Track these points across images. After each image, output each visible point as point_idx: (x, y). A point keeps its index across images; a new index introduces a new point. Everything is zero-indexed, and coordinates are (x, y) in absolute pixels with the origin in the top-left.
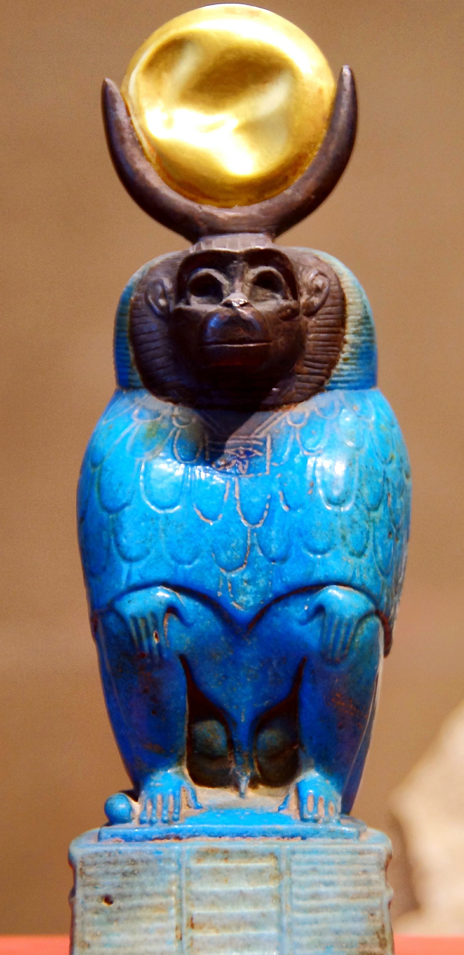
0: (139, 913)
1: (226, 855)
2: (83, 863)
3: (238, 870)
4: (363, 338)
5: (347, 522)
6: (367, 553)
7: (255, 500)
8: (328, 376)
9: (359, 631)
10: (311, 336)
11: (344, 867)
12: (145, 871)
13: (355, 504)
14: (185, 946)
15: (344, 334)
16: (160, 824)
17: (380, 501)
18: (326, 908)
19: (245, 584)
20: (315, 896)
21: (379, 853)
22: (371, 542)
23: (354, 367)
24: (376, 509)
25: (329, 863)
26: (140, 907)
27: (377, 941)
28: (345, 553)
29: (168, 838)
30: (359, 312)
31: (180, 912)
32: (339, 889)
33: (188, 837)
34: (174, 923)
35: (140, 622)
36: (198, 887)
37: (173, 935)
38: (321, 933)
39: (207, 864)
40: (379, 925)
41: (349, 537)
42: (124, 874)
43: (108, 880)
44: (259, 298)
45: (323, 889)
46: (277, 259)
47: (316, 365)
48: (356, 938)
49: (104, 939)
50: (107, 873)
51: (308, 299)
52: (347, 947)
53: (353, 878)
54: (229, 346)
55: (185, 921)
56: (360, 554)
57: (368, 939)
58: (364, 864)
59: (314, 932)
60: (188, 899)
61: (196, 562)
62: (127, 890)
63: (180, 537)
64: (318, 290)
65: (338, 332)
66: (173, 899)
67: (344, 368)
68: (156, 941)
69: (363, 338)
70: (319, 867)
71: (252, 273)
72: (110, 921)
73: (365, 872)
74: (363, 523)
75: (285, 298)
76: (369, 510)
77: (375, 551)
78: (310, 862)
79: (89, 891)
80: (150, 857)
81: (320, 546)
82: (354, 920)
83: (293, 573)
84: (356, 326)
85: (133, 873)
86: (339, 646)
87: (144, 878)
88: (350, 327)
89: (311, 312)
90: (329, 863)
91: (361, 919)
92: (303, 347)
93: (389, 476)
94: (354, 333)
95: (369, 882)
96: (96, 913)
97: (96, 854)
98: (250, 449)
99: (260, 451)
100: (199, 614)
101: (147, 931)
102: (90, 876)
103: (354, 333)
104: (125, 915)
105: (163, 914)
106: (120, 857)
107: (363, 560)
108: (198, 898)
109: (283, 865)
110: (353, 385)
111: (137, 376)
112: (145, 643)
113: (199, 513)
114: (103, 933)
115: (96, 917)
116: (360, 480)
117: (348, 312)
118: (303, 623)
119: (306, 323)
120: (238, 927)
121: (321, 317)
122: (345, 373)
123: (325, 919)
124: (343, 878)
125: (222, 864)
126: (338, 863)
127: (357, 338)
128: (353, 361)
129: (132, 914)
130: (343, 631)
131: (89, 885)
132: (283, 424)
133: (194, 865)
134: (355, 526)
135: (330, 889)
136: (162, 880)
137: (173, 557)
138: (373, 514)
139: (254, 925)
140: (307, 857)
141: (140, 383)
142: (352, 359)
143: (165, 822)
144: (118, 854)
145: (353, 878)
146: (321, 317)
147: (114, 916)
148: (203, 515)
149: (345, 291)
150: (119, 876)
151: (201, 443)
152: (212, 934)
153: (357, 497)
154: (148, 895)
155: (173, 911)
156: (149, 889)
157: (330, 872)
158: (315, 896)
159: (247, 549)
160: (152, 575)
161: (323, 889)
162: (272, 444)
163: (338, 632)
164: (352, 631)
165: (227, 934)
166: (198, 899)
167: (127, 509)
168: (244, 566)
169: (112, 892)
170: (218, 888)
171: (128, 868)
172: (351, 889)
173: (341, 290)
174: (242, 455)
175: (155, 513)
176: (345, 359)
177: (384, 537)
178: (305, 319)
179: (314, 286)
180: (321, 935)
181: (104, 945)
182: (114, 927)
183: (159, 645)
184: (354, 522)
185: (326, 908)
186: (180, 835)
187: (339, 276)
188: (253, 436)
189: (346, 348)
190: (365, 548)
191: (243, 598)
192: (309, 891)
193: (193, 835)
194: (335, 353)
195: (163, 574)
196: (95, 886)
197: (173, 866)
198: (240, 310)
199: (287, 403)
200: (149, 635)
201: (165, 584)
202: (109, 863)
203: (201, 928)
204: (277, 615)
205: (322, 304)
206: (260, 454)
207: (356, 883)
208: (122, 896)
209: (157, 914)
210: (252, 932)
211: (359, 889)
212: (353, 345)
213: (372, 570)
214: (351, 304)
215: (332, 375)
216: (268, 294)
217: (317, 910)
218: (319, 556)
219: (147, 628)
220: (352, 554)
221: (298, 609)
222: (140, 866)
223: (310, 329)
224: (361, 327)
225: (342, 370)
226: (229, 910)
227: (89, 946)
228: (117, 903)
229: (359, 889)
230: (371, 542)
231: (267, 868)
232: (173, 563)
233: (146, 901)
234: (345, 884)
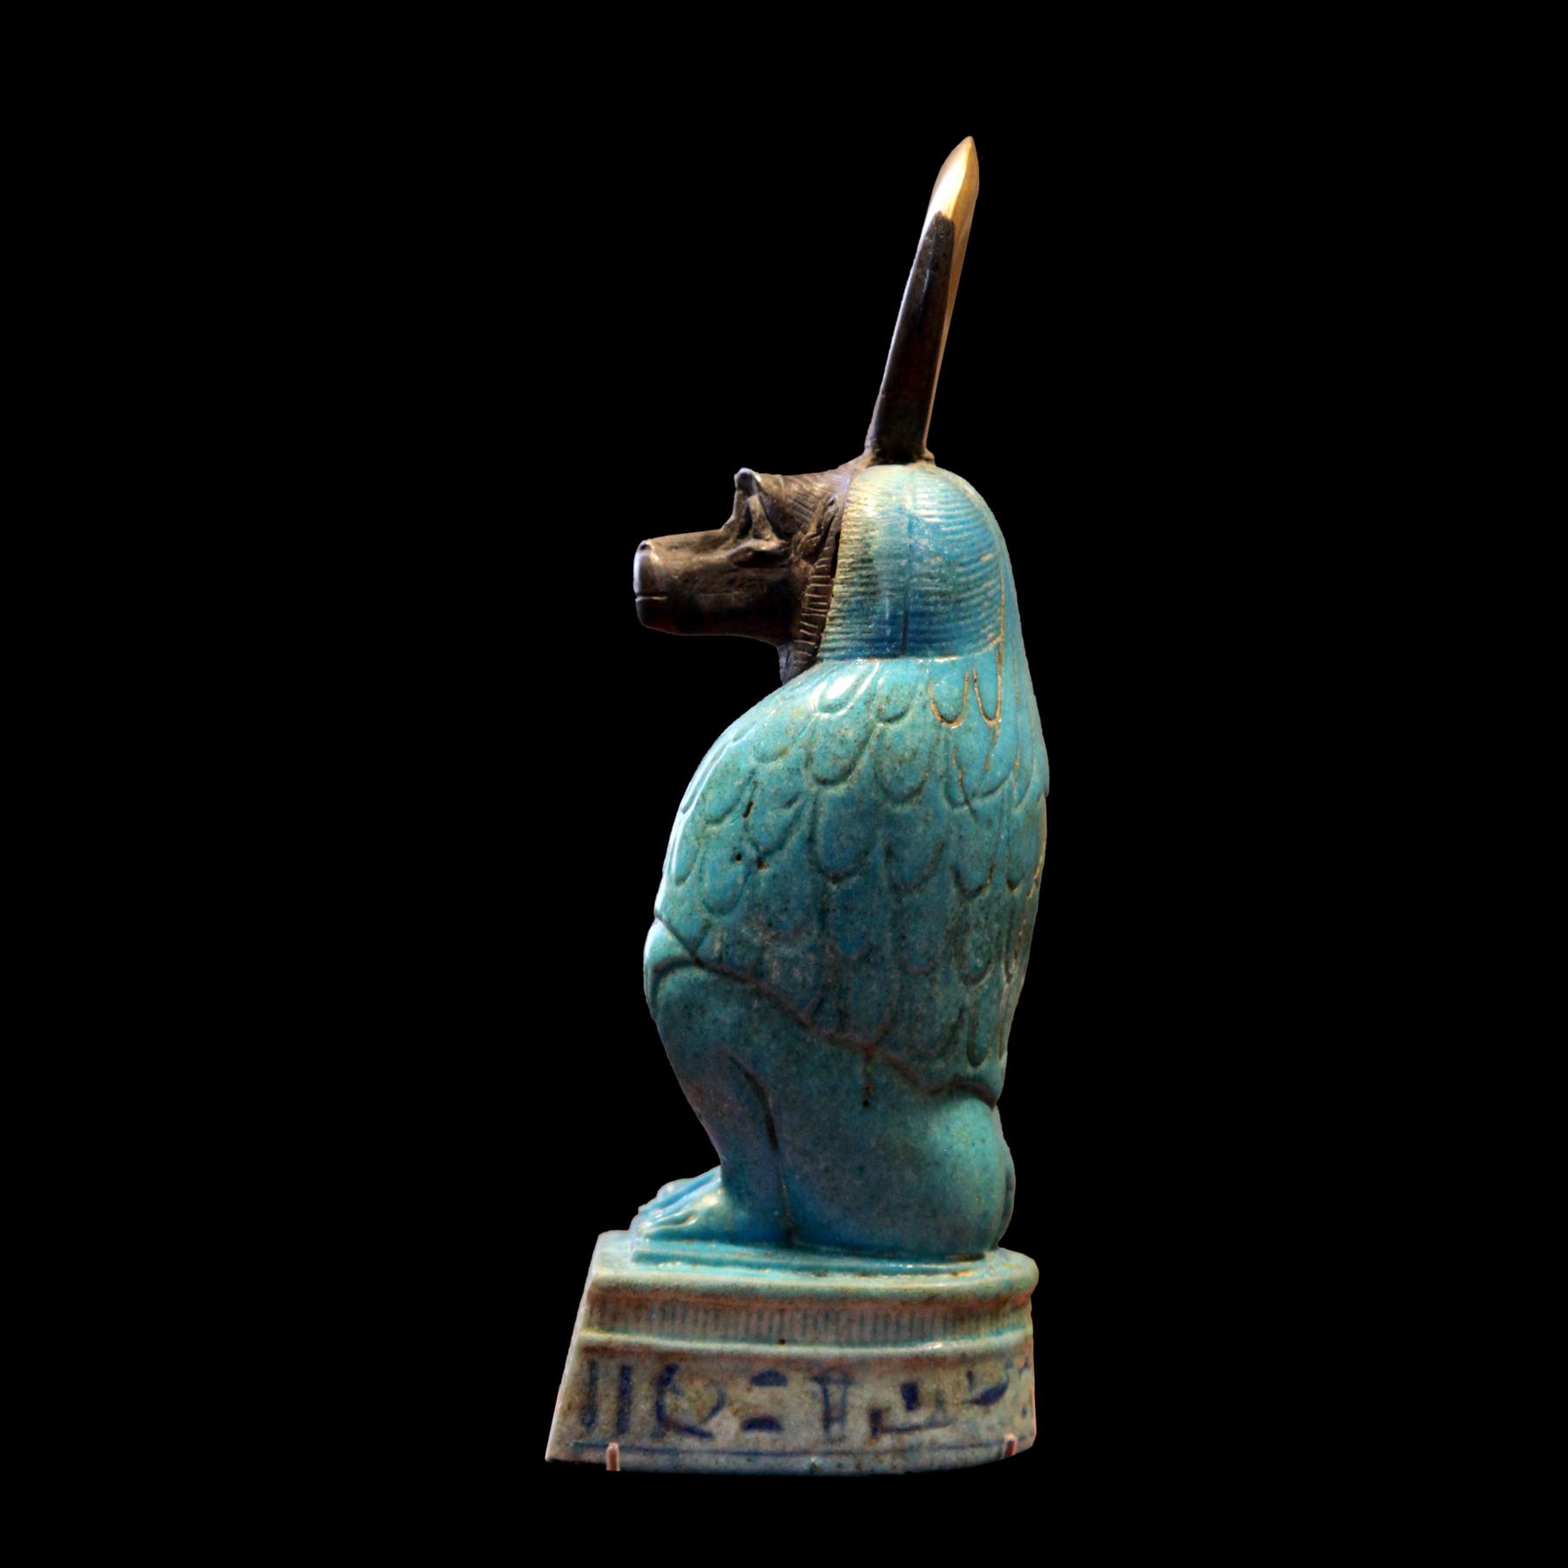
4: (853, 589)
8: (819, 642)
17: (729, 811)
22: (696, 867)
24: (718, 821)
67: (833, 634)
69: (853, 589)
76: (708, 822)
77: (701, 879)
88: (839, 576)
93: (761, 777)
107: (681, 889)
176: (832, 618)
177: (720, 861)
178: (804, 564)
212: (840, 599)
213: (687, 904)
230: (696, 867)
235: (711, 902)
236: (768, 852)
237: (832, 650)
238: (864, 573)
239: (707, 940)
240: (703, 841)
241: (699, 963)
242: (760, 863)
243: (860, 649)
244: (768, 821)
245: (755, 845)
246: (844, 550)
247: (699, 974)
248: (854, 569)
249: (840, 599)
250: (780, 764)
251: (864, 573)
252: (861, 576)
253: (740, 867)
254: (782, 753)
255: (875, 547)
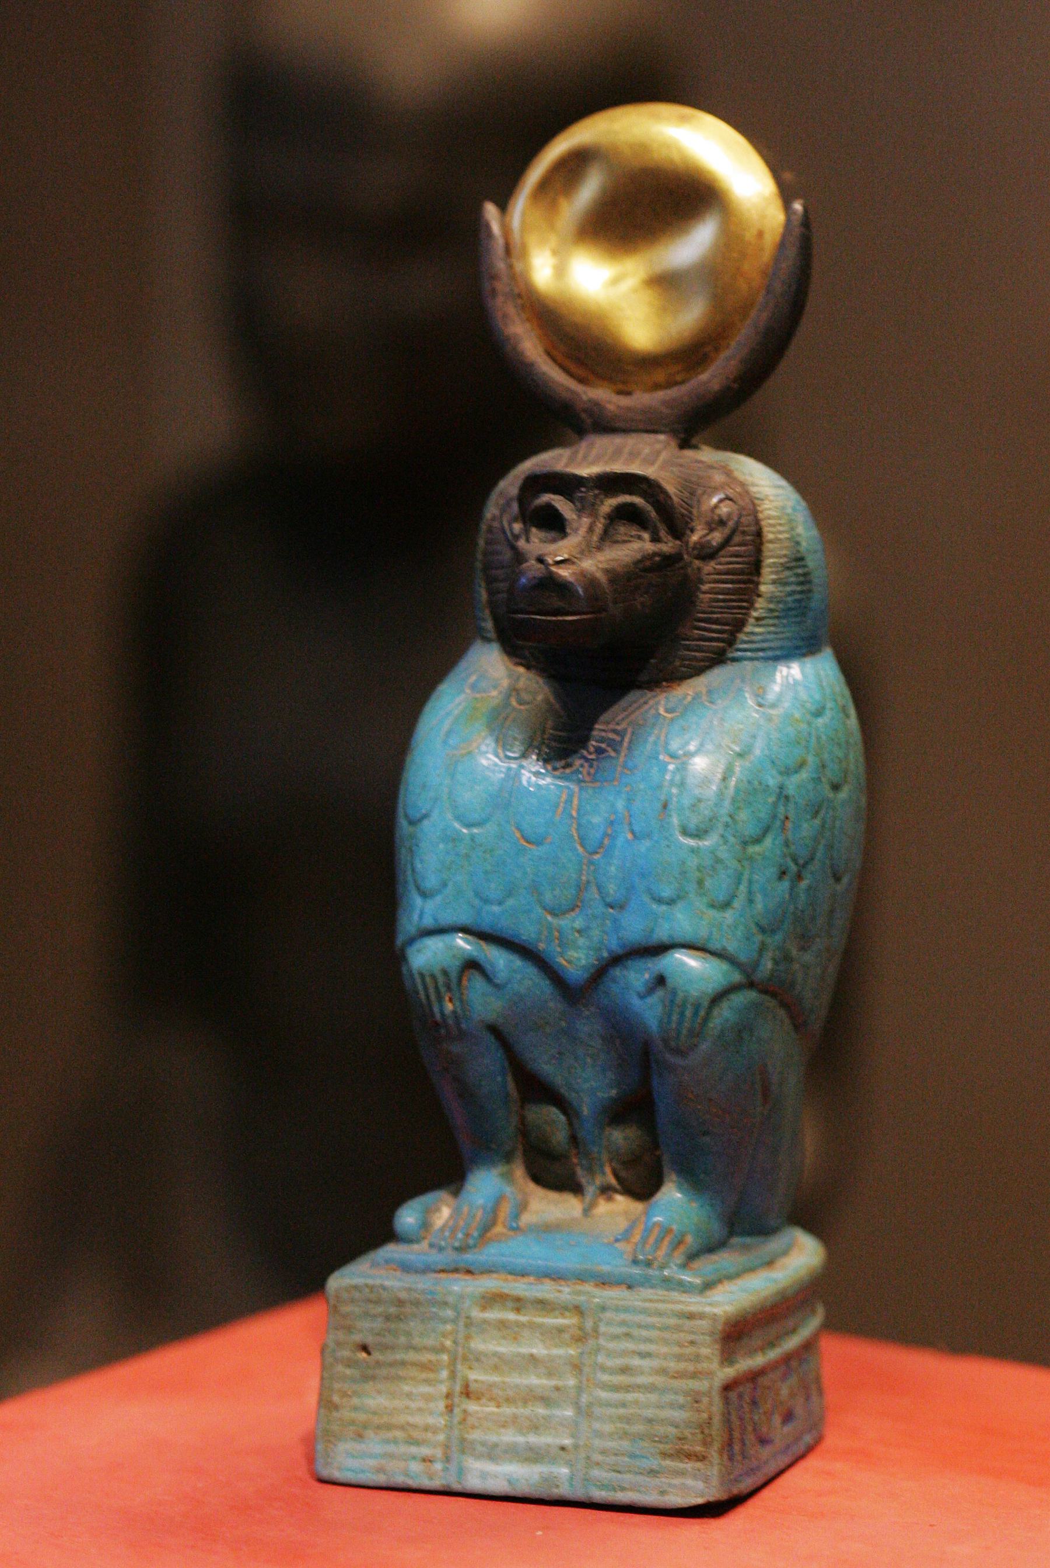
0: (401, 1372)
1: (519, 1303)
2: (337, 1297)
3: (532, 1326)
4: (789, 589)
5: (709, 862)
6: (737, 904)
7: (596, 820)
9: (716, 1012)
10: (705, 587)
11: (667, 1335)
12: (415, 1316)
13: (722, 836)
14: (456, 1420)
15: (758, 584)
16: (450, 1251)
17: (766, 830)
18: (638, 1387)
19: (577, 935)
20: (625, 1370)
21: (714, 1318)
22: (743, 888)
23: (772, 629)
24: (758, 840)
25: (647, 1327)
26: (403, 1363)
27: (700, 1436)
28: (700, 903)
29: (456, 1270)
30: (784, 552)
31: (453, 1375)
32: (655, 1363)
33: (482, 1273)
34: (444, 1389)
35: (428, 980)
36: (478, 1344)
37: (441, 1405)
38: (628, 1420)
39: (493, 1315)
40: (705, 1416)
41: (708, 883)
42: (388, 1318)
43: (366, 1324)
44: (619, 538)
45: (636, 1362)
46: (644, 486)
47: (714, 627)
48: (672, 1431)
49: (355, 1401)
50: (366, 1314)
51: (705, 536)
52: (660, 1442)
53: (676, 1350)
54: (538, 617)
55: (458, 1388)
56: (726, 905)
57: (687, 1433)
58: (693, 1333)
59: (621, 1418)
60: (465, 1359)
61: (510, 902)
62: (388, 1339)
63: (489, 868)
64: (722, 523)
65: (750, 581)
66: (445, 1357)
68: (420, 1410)
69: (789, 589)
70: (636, 1332)
71: (609, 504)
72: (366, 1378)
73: (692, 1343)
74: (733, 864)
75: (656, 539)
76: (745, 843)
77: (751, 901)
78: (623, 1323)
79: (341, 1336)
80: (422, 1298)
81: (666, 892)
82: (672, 1405)
83: (634, 928)
84: (776, 573)
85: (398, 1318)
86: (684, 1032)
87: (413, 1325)
88: (768, 574)
89: (707, 553)
90: (647, 1327)
91: (682, 1407)
92: (693, 603)
93: (791, 791)
94: (774, 582)
95: (697, 1358)
96: (349, 1366)
97: (356, 1287)
98: (603, 746)
99: (615, 750)
100: (515, 971)
101: (409, 1395)
102: (345, 1316)
103: (774, 582)
104: (384, 1372)
105: (431, 1376)
106: (385, 1295)
107: (729, 916)
108: (476, 1359)
109: (589, 1324)
110: (770, 653)
111: (489, 625)
112: (436, 1010)
113: (518, 835)
114: (355, 1393)
115: (348, 1372)
116: (734, 800)
117: (766, 553)
118: (642, 997)
119: (699, 569)
120: (525, 1402)
121: (723, 560)
122: (759, 638)
123: (636, 1402)
124: (664, 1350)
125: (511, 1316)
126: (659, 1329)
127: (781, 589)
128: (771, 622)
129: (393, 1371)
130: (688, 1013)
131: (343, 1327)
132: (653, 711)
133: (476, 1314)
134: (719, 866)
135: (645, 1363)
136: (434, 1331)
137: (477, 894)
138: (752, 849)
139: (545, 1401)
140: (623, 1316)
141: (492, 635)
142: (770, 618)
143: (456, 1249)
144: (381, 1291)
145: (676, 1350)
146: (723, 560)
147: (370, 1372)
148: (523, 837)
149: (763, 523)
150: (380, 1319)
151: (539, 733)
152: (492, 1409)
153: (727, 825)
154: (416, 1349)
155: (444, 1374)
156: (417, 1341)
157: (649, 1340)
158: (625, 1370)
159: (581, 888)
160: (448, 917)
161: (636, 1362)
162: (630, 742)
163: (682, 1014)
164: (702, 1013)
165: (508, 1410)
166: (478, 1360)
167: (426, 823)
168: (577, 910)
169: (370, 1340)
170: (505, 1348)
171: (392, 1310)
172: (673, 1365)
173: (757, 522)
174: (590, 753)
175: (458, 832)
176: (758, 619)
179: (716, 518)
180: (628, 1423)
181: (355, 1409)
182: (369, 1386)
183: (454, 1012)
184: (718, 861)
185: (638, 1387)
186: (472, 1268)
187: (756, 502)
188: (611, 726)
189: (760, 603)
190: (733, 896)
191: (572, 954)
192: (619, 1362)
193: (489, 1270)
194: (743, 611)
195: (464, 917)
196: (349, 1329)
197: (449, 1313)
198: (554, 569)
199: (667, 680)
200: (440, 998)
201: (465, 930)
202: (370, 1301)
203: (478, 1399)
204: (614, 980)
205: (727, 542)
206: (613, 754)
207: (679, 1358)
208: (385, 1348)
209: (424, 1375)
210: (541, 1411)
211: (682, 1366)
212: (770, 600)
213: (741, 928)
214: (771, 541)
215: (738, 641)
216: (633, 533)
217: (628, 1388)
218: (664, 908)
219: (436, 988)
220: (712, 906)
221: (636, 976)
222: (408, 1309)
223: (705, 578)
224: (787, 573)
225: (752, 633)
226: (515, 1379)
227: (336, 1407)
228: (377, 1356)
229: (682, 1366)
230: (743, 888)
231: (569, 1327)
232: (477, 902)
233: (412, 1356)
234: (665, 1357)
235: (764, 922)
236: (805, 864)
237: (762, 650)
238: (800, 571)
239: (763, 961)
240: (746, 863)
241: (751, 985)
242: (799, 877)
243: (797, 648)
244: (805, 834)
245: (795, 861)
246: (768, 548)
247: (752, 995)
248: (788, 568)
249: (770, 600)
250: (804, 775)
251: (800, 571)
252: (797, 575)
253: (786, 884)
254: (802, 765)
255: (804, 544)
